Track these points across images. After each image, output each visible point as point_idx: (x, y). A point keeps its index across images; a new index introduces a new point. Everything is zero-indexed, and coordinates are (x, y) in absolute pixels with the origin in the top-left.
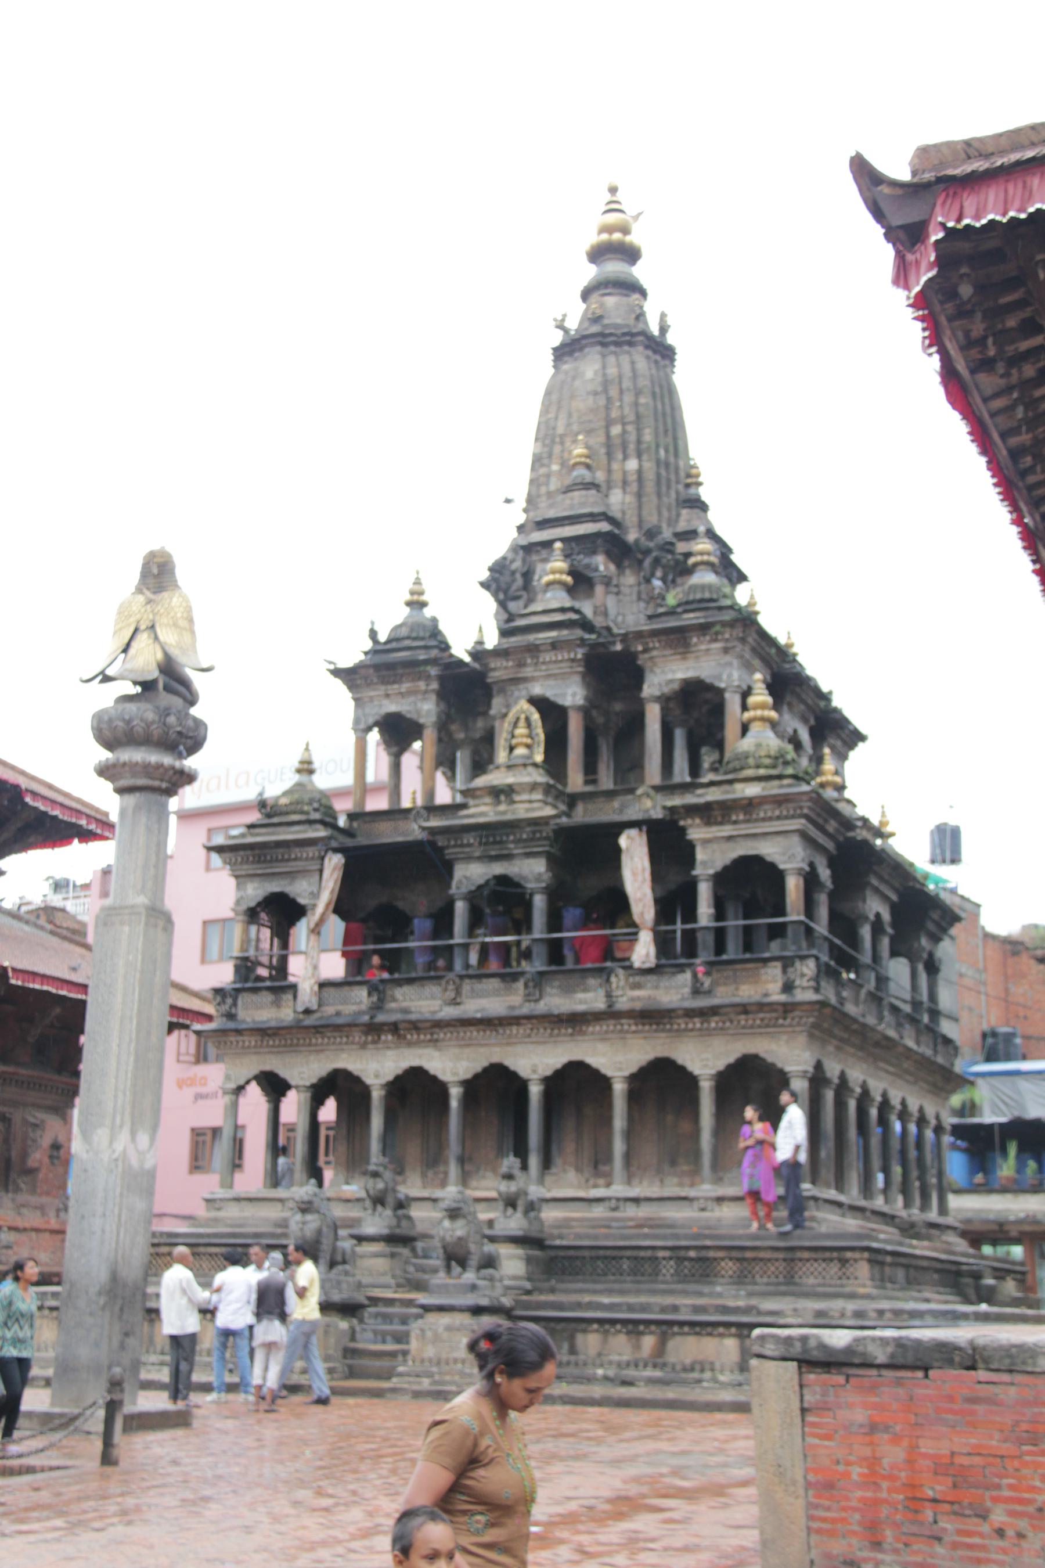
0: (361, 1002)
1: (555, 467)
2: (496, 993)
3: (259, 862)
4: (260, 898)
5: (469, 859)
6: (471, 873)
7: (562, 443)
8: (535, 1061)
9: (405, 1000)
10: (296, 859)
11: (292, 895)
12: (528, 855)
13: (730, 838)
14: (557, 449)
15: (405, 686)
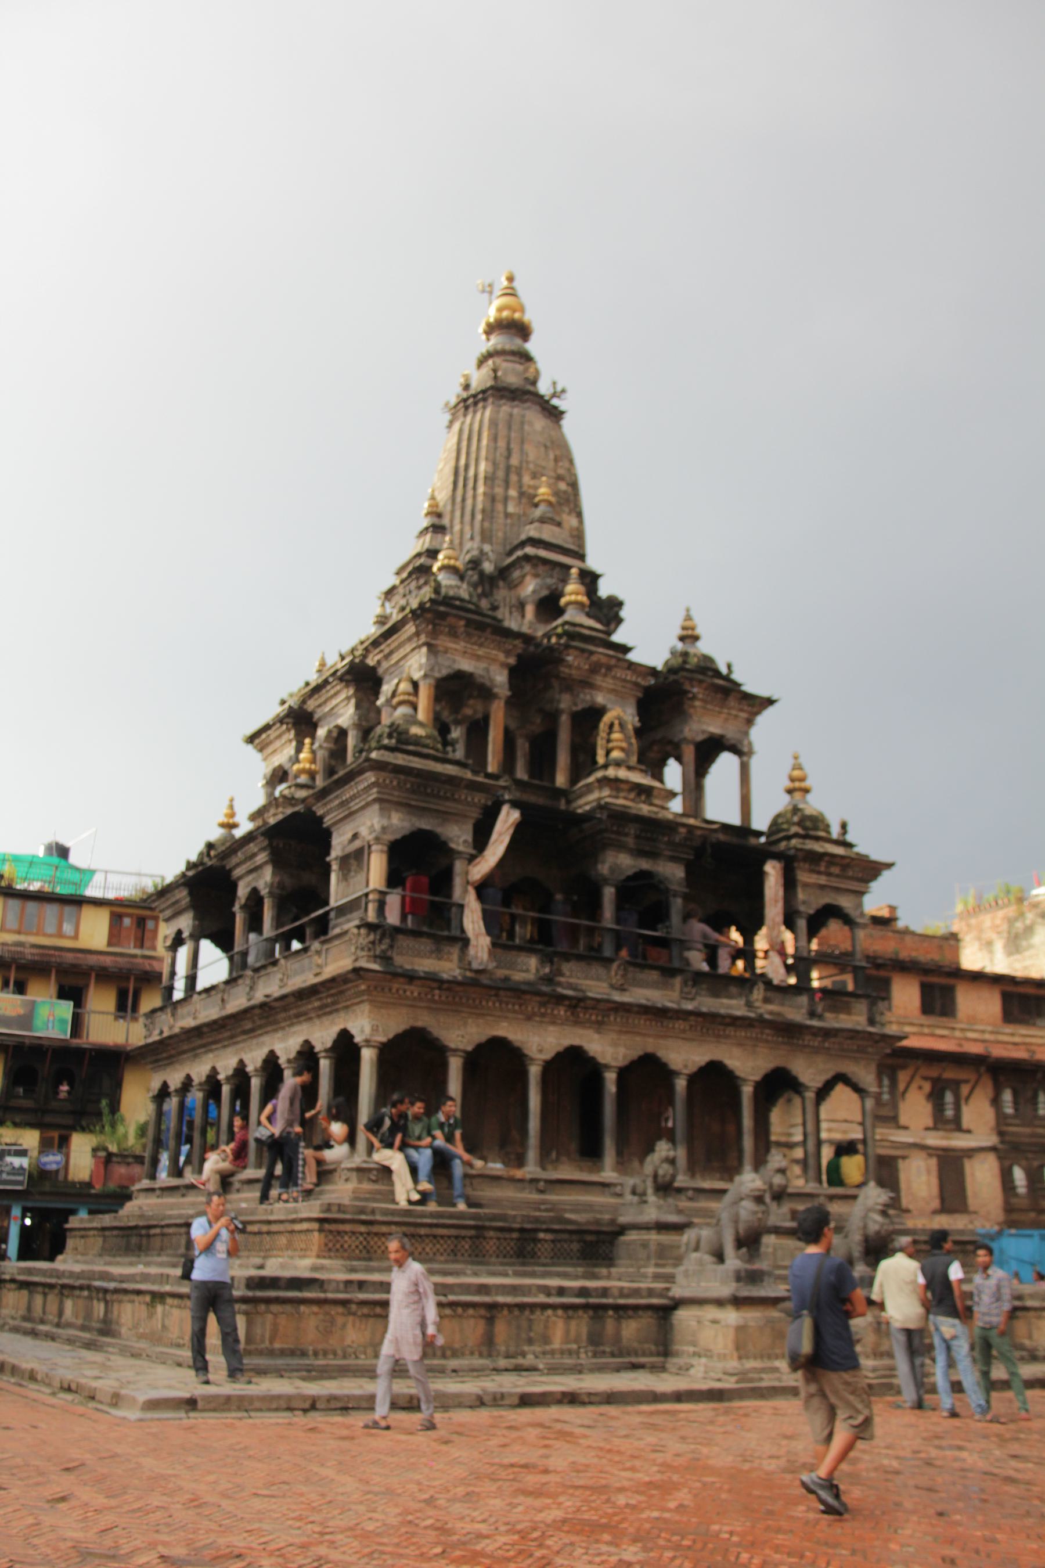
0: (527, 971)
1: (513, 493)
2: (654, 985)
3: (413, 792)
4: (406, 832)
5: (621, 847)
6: (619, 862)
7: (519, 475)
8: (685, 1056)
9: (571, 976)
10: (455, 800)
11: (443, 838)
12: (673, 859)
13: (822, 887)
14: (514, 478)
15: (481, 652)
